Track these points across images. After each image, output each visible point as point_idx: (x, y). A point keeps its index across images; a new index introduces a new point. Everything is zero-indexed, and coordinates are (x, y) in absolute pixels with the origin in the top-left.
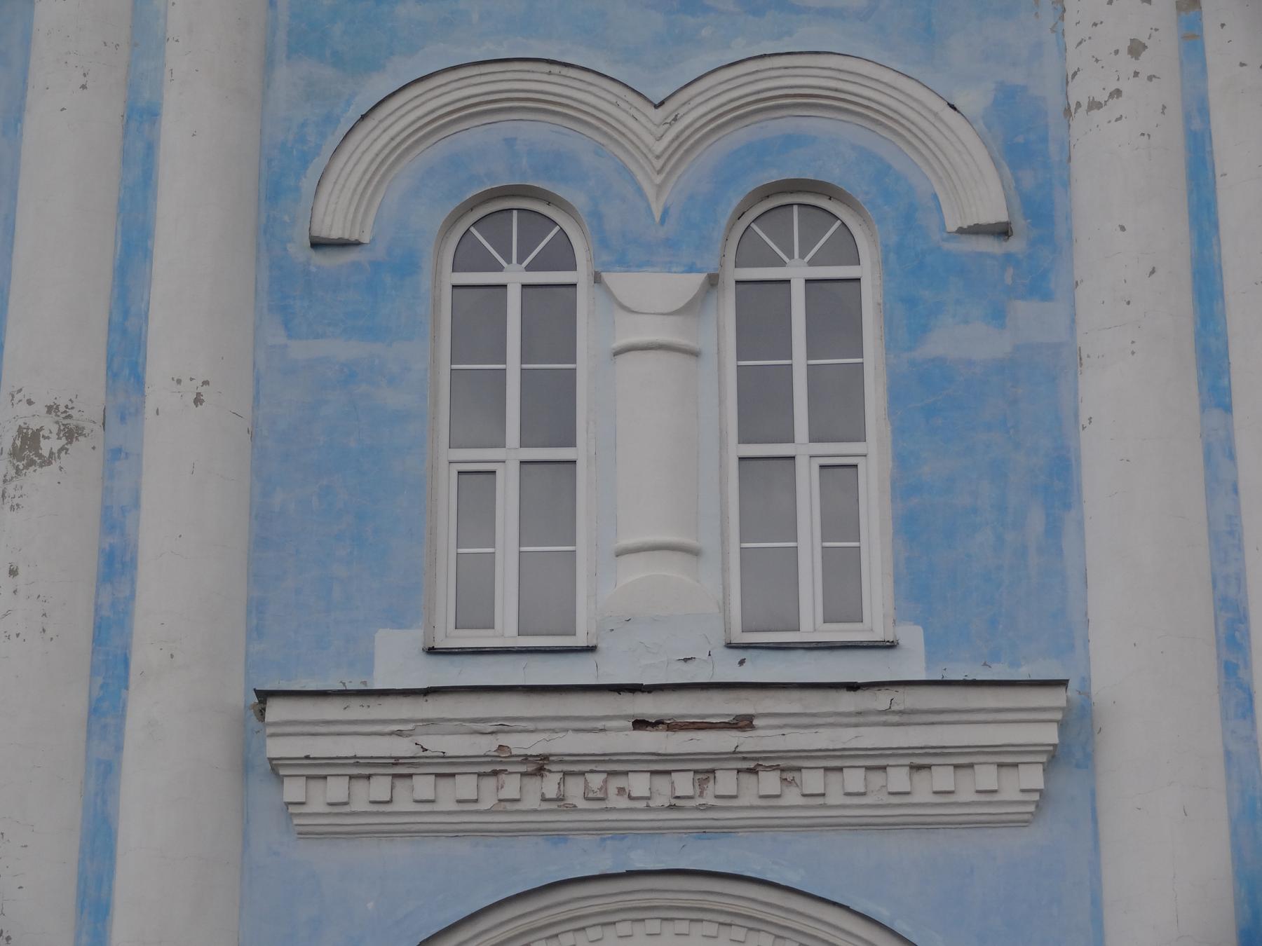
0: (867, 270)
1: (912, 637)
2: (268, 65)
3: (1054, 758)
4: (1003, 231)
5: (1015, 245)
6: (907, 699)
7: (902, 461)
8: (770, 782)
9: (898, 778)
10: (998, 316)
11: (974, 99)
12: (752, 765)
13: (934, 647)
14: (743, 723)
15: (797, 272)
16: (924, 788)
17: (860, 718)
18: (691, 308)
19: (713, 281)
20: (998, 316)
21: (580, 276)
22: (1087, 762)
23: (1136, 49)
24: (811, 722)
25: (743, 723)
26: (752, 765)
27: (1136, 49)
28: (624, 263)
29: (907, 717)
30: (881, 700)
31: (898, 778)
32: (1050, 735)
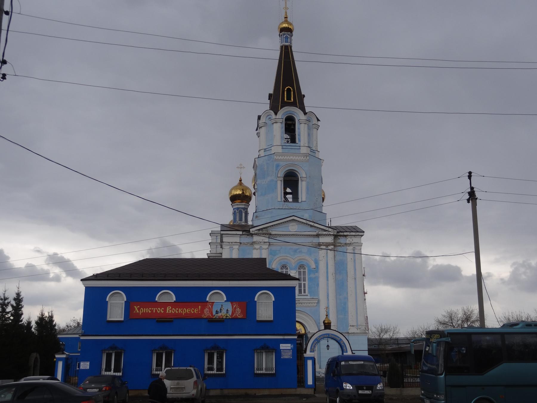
0: (306, 270)
1: (309, 295)
2: (269, 255)
3: (317, 303)
4: (315, 268)
5: (316, 269)
6: (308, 300)
7: (309, 284)
8: (300, 304)
9: (308, 304)
10: (314, 274)
11: (313, 259)
12: (299, 303)
13: (310, 296)
14: (299, 301)
15: (302, 270)
16: (309, 305)
17: (306, 301)
18: (296, 273)
19: (297, 271)
20: (314, 274)
21: (288, 270)
22: (319, 303)
23: (324, 257)
24: (303, 301)
25: (299, 301)
26: (299, 303)
27: (324, 257)
28: (291, 270)
29: (309, 301)
30: (307, 300)
31: (308, 304)
32: (317, 302)
